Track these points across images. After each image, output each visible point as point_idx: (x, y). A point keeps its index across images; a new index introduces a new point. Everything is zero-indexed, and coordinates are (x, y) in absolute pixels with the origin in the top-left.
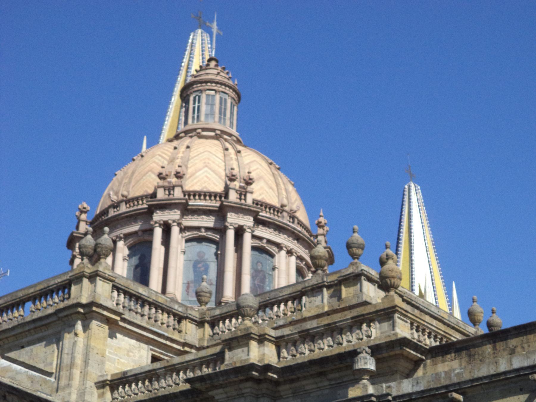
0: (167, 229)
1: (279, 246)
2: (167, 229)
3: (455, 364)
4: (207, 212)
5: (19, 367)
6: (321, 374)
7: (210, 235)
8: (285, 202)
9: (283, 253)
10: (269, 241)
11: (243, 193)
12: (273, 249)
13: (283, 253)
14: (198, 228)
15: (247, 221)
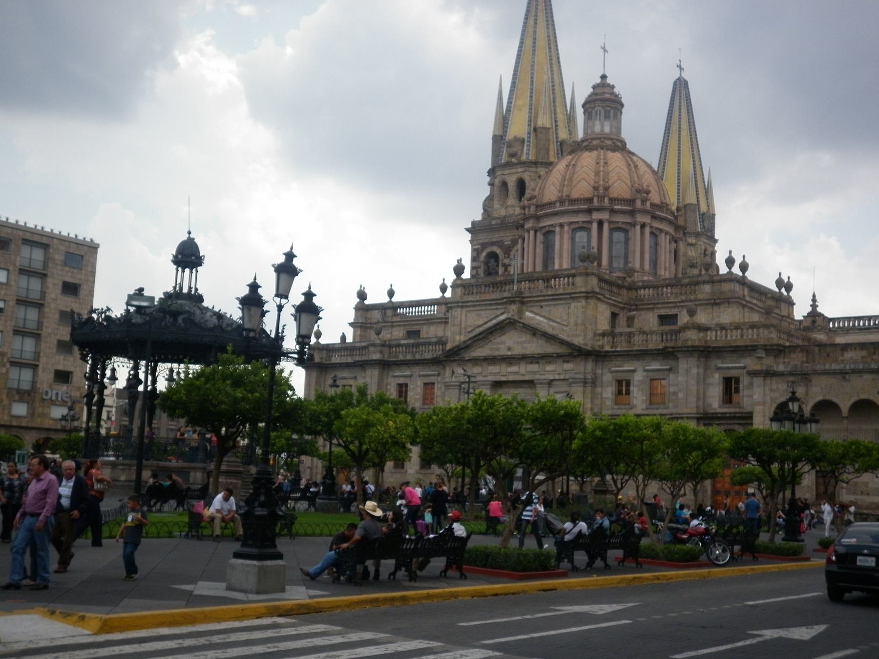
0: (600, 223)
1: (661, 230)
2: (600, 223)
3: (800, 355)
4: (623, 212)
5: (541, 319)
6: (732, 351)
7: (624, 226)
8: (664, 201)
9: (663, 234)
10: (656, 228)
11: (644, 201)
12: (657, 233)
13: (663, 234)
14: (618, 222)
15: (647, 219)
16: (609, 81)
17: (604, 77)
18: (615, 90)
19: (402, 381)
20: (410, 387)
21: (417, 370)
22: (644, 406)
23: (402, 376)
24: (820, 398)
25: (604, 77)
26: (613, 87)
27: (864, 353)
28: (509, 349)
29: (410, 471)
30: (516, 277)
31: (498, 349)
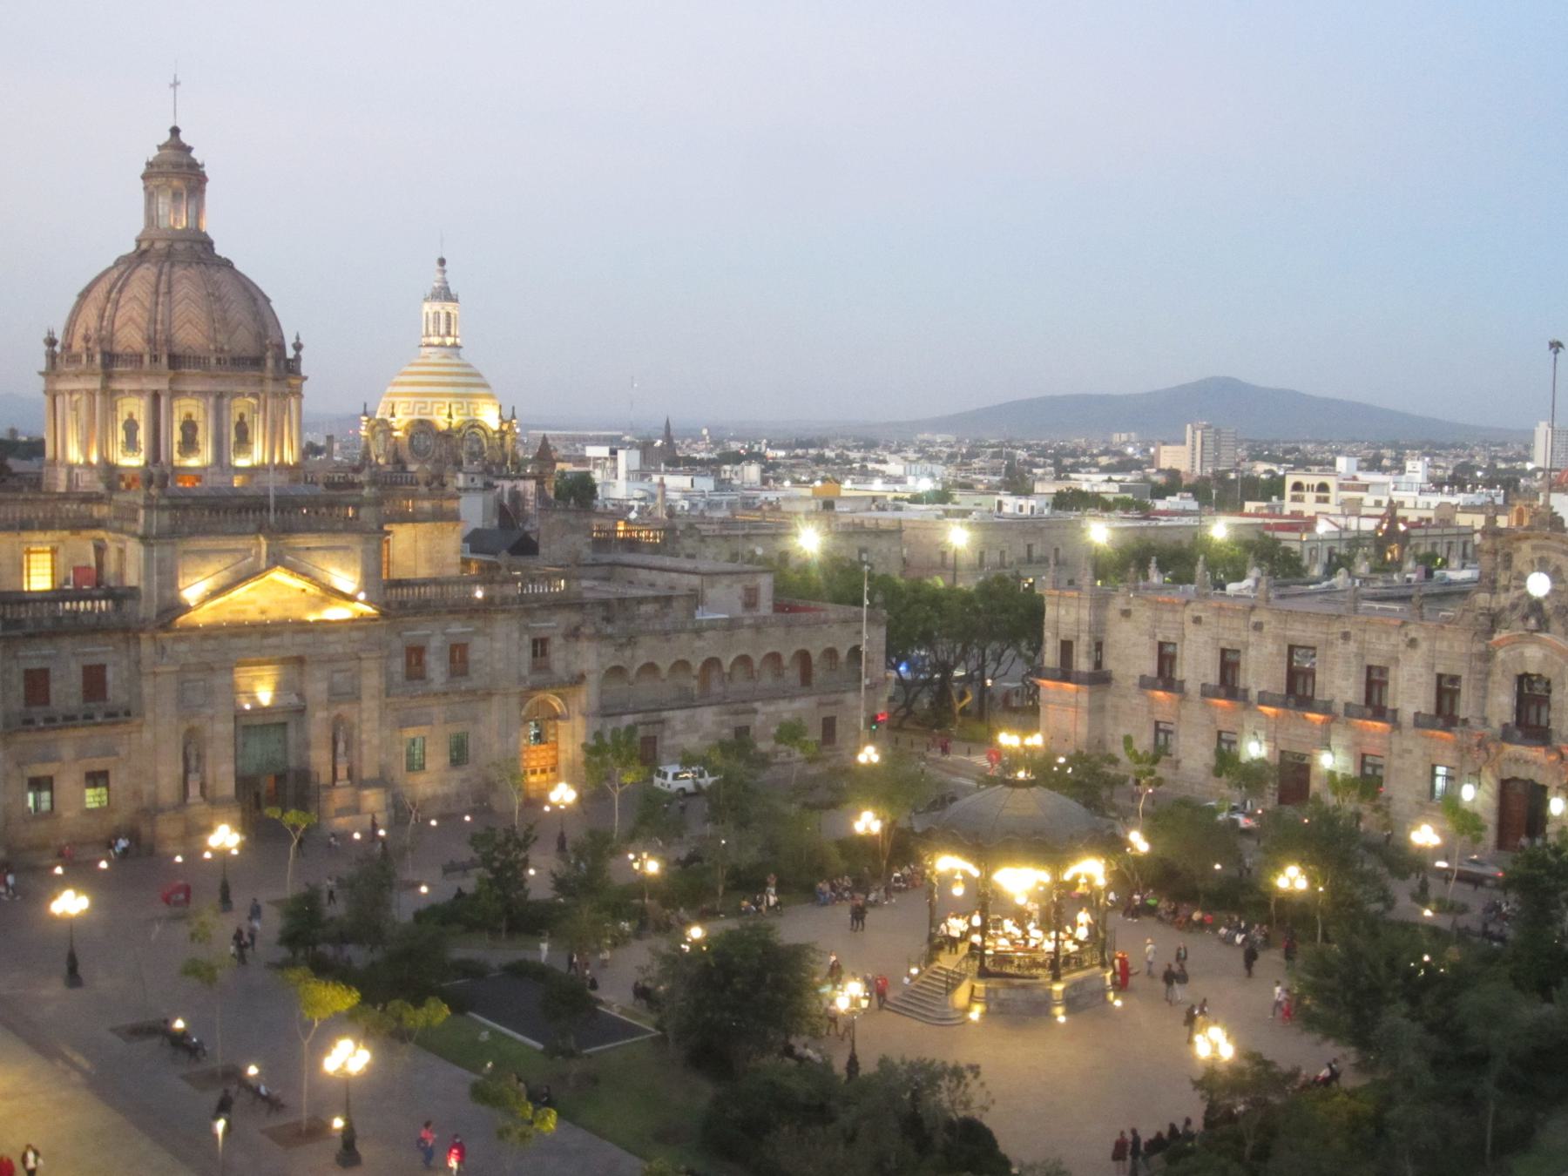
16: (185, 138)
17: (175, 131)
18: (194, 154)
19: (35, 664)
20: (55, 674)
21: (67, 644)
22: (443, 680)
23: (37, 657)
24: (644, 661)
25: (175, 131)
26: (189, 149)
27: (657, 606)
28: (263, 612)
29: (67, 814)
30: (272, 501)
31: (244, 612)
